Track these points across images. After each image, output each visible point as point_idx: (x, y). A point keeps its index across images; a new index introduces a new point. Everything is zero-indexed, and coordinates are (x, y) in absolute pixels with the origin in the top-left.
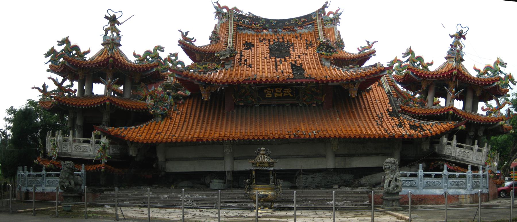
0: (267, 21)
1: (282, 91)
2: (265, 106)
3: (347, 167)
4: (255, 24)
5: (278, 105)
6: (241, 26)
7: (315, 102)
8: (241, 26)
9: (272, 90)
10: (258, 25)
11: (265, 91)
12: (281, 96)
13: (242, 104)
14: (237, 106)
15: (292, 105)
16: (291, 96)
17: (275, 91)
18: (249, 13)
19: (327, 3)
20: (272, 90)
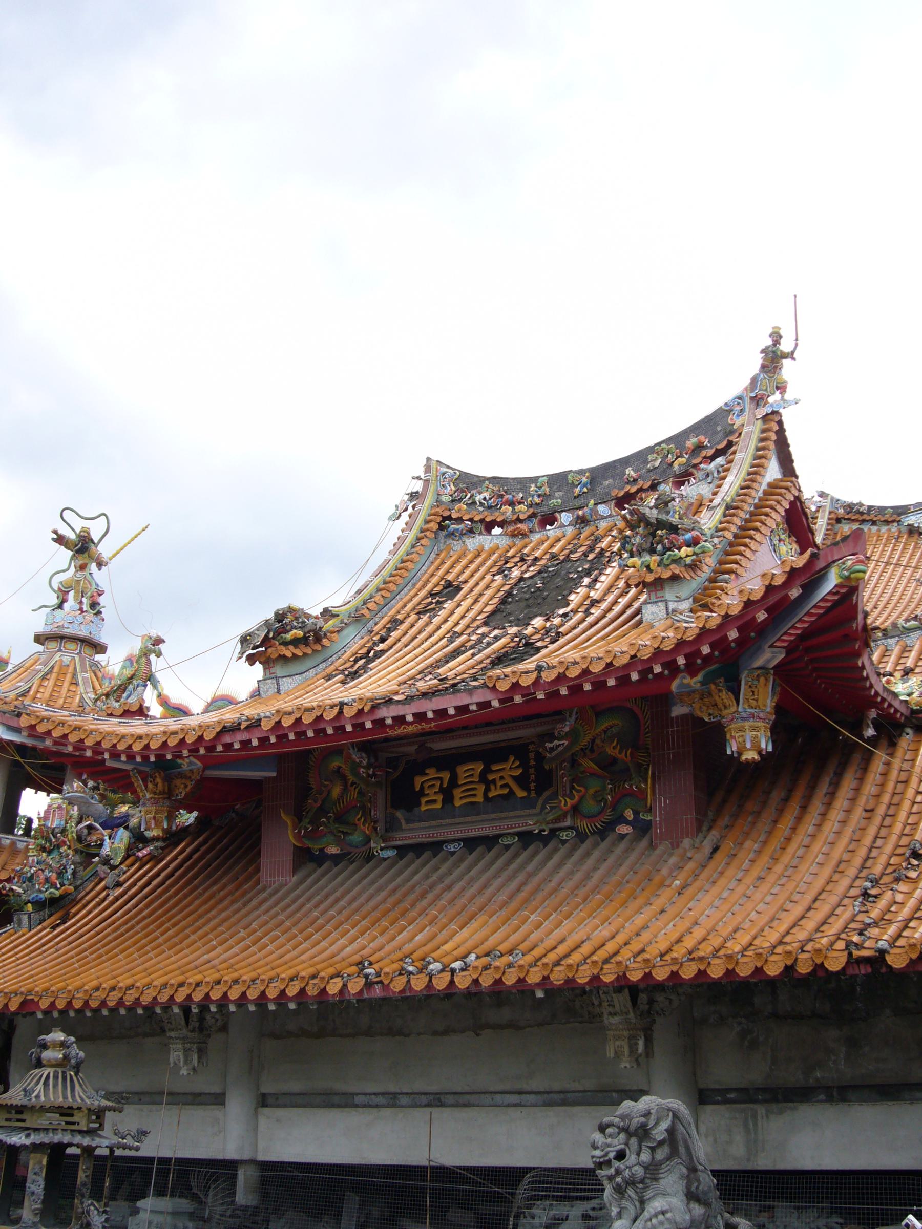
0: (559, 480)
1: (483, 778)
2: (418, 849)
3: (763, 1163)
4: (512, 504)
5: (470, 844)
6: (460, 520)
7: (629, 814)
8: (460, 520)
9: (446, 776)
10: (522, 507)
11: (418, 781)
12: (480, 799)
13: (333, 850)
14: (305, 858)
15: (526, 838)
16: (521, 794)
17: (454, 783)
18: (822, 495)
19: (776, 337)
20: (446, 776)
